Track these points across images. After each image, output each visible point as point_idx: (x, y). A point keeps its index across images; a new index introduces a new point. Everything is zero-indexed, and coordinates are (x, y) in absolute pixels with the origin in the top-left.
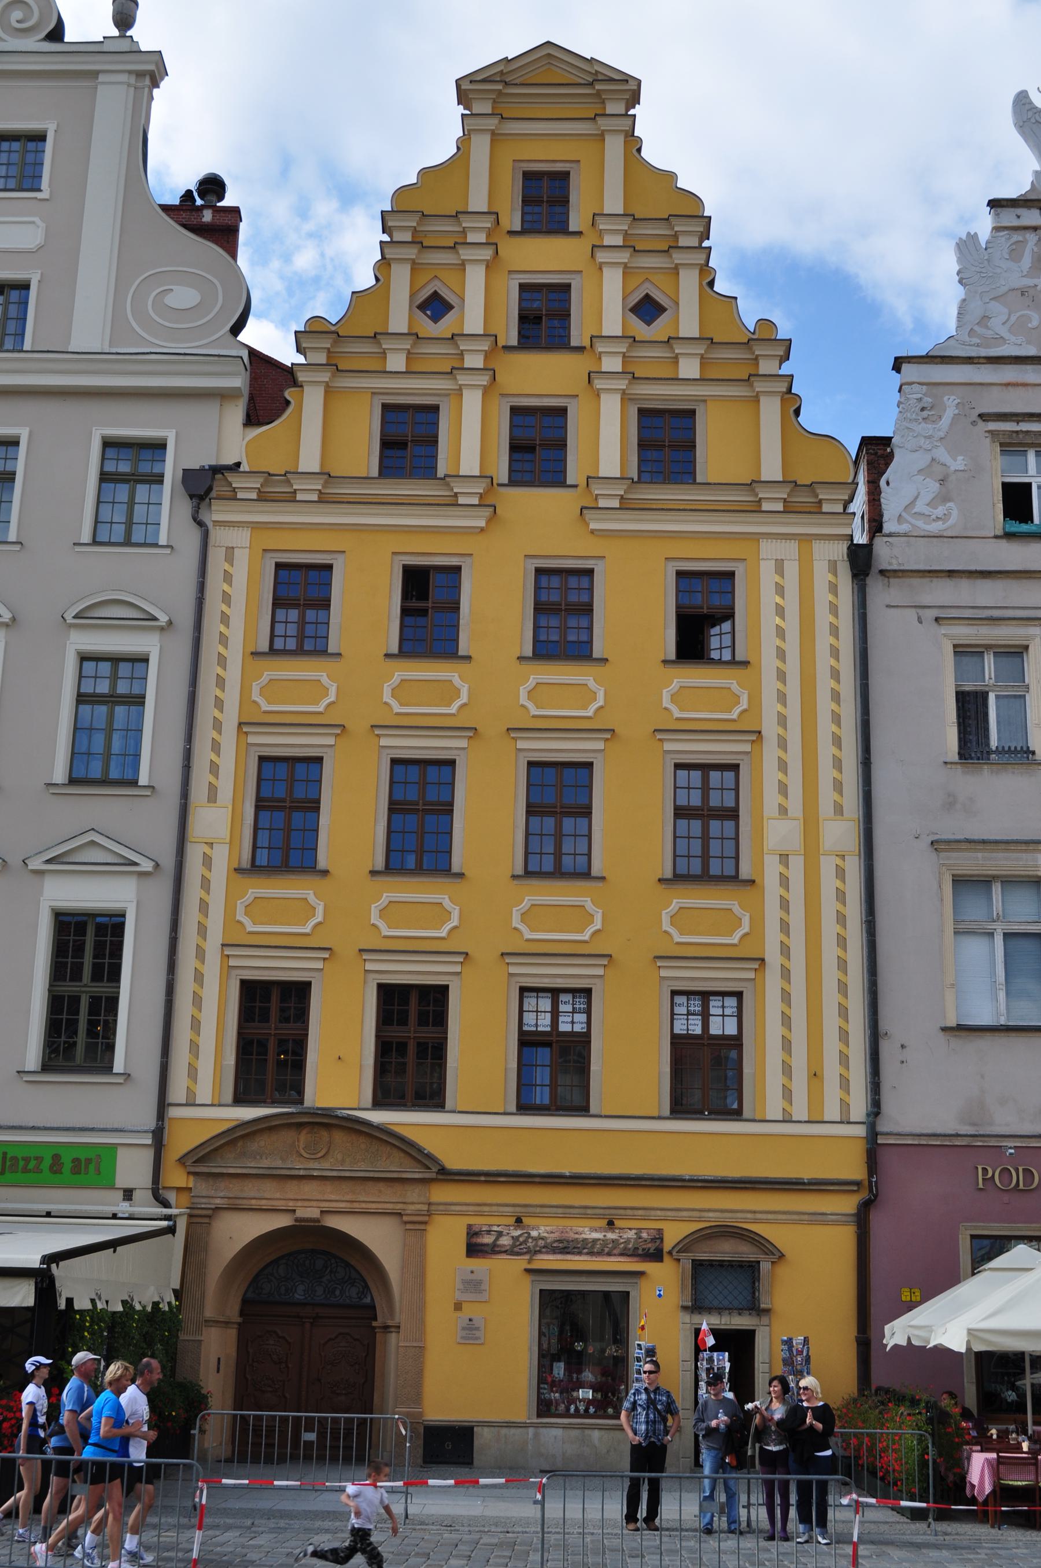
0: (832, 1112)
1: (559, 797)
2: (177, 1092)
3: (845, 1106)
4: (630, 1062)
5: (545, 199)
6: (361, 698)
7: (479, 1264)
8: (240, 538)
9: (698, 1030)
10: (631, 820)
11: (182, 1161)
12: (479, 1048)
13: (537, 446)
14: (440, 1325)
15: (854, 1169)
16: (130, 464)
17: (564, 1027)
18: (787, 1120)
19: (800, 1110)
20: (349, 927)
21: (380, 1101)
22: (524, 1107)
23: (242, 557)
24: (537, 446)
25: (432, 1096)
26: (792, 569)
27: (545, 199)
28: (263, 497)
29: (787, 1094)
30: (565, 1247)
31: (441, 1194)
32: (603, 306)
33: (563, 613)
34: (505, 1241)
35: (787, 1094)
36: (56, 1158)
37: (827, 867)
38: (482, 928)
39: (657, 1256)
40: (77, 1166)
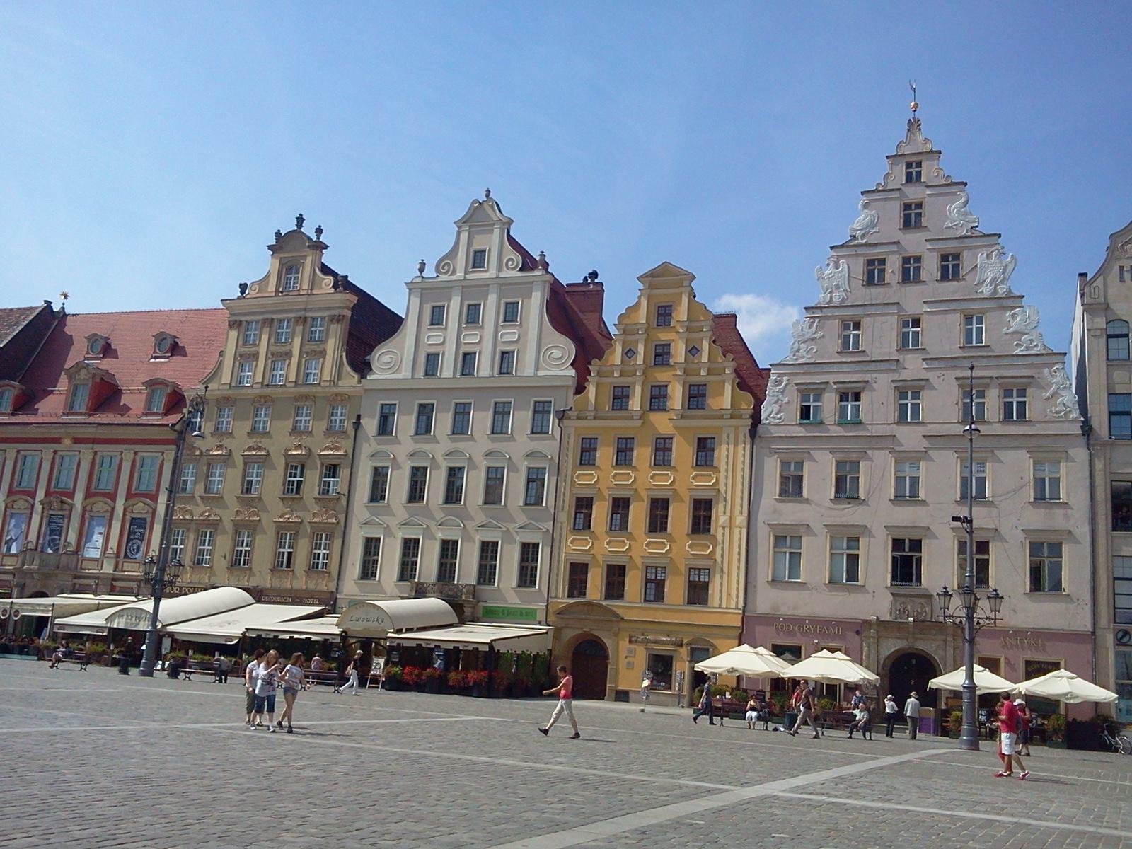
0: (733, 606)
1: (659, 509)
2: (552, 594)
3: (737, 603)
4: (676, 589)
5: (663, 315)
6: (605, 478)
7: (632, 646)
8: (572, 431)
9: (697, 579)
10: (679, 517)
11: (553, 613)
12: (633, 584)
13: (658, 398)
14: (623, 663)
15: (740, 625)
16: (541, 410)
17: (659, 578)
18: (720, 607)
19: (724, 605)
20: (600, 546)
21: (607, 598)
22: (646, 601)
23: (572, 436)
24: (658, 398)
25: (621, 596)
26: (732, 436)
27: (663, 315)
28: (578, 418)
29: (721, 599)
30: (656, 642)
31: (622, 625)
32: (679, 352)
33: (662, 450)
34: (639, 640)
35: (721, 599)
36: (521, 612)
37: (736, 531)
38: (638, 547)
39: (681, 645)
40: (527, 614)
